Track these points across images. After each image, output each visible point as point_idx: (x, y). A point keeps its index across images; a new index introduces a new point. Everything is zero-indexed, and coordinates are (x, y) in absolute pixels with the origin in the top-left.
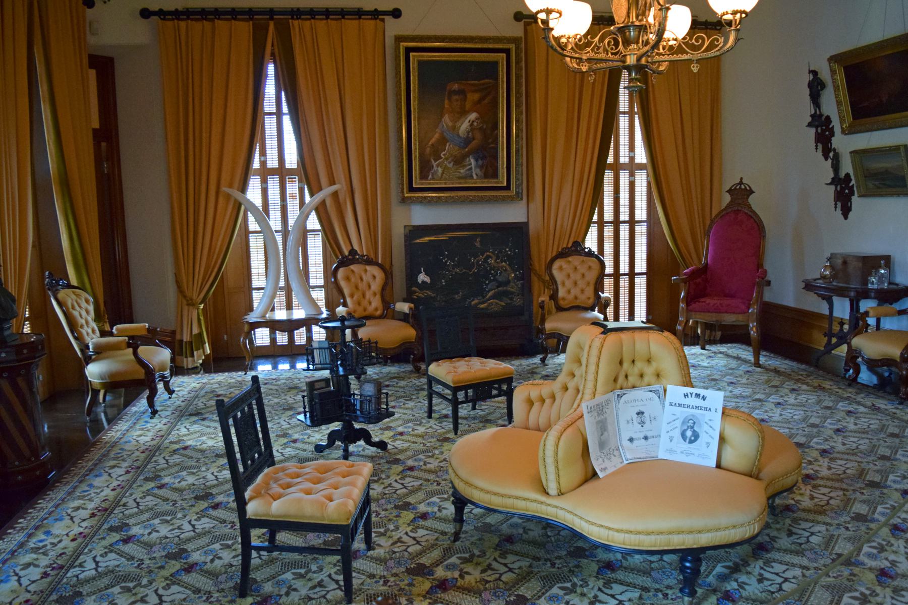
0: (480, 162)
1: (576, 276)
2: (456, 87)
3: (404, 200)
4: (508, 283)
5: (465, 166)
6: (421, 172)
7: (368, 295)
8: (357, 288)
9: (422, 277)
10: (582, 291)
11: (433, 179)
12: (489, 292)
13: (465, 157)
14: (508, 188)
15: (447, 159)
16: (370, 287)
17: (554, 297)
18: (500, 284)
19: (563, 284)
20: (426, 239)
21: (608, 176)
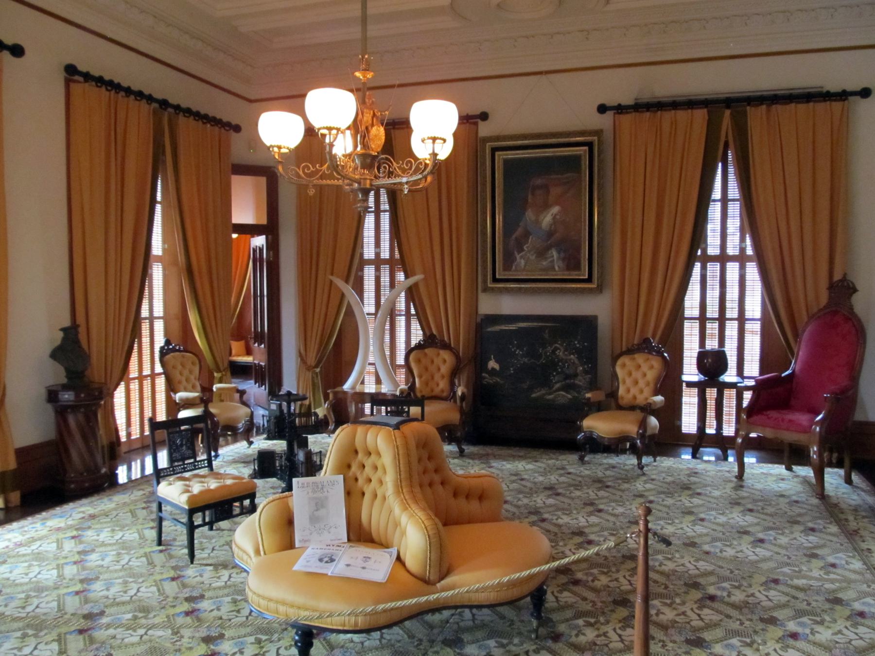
0: (562, 255)
1: (637, 375)
2: (539, 181)
3: (486, 290)
4: (576, 375)
5: (546, 259)
6: (504, 265)
7: (437, 377)
8: (426, 369)
9: (493, 364)
10: (641, 391)
11: (516, 270)
12: (556, 383)
13: (549, 248)
14: (589, 280)
15: (529, 251)
16: (439, 369)
17: (613, 395)
18: (568, 377)
19: (624, 382)
20: (497, 328)
21: (697, 267)
